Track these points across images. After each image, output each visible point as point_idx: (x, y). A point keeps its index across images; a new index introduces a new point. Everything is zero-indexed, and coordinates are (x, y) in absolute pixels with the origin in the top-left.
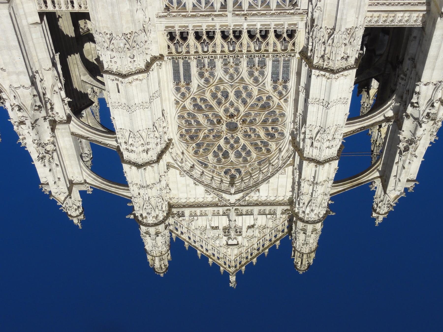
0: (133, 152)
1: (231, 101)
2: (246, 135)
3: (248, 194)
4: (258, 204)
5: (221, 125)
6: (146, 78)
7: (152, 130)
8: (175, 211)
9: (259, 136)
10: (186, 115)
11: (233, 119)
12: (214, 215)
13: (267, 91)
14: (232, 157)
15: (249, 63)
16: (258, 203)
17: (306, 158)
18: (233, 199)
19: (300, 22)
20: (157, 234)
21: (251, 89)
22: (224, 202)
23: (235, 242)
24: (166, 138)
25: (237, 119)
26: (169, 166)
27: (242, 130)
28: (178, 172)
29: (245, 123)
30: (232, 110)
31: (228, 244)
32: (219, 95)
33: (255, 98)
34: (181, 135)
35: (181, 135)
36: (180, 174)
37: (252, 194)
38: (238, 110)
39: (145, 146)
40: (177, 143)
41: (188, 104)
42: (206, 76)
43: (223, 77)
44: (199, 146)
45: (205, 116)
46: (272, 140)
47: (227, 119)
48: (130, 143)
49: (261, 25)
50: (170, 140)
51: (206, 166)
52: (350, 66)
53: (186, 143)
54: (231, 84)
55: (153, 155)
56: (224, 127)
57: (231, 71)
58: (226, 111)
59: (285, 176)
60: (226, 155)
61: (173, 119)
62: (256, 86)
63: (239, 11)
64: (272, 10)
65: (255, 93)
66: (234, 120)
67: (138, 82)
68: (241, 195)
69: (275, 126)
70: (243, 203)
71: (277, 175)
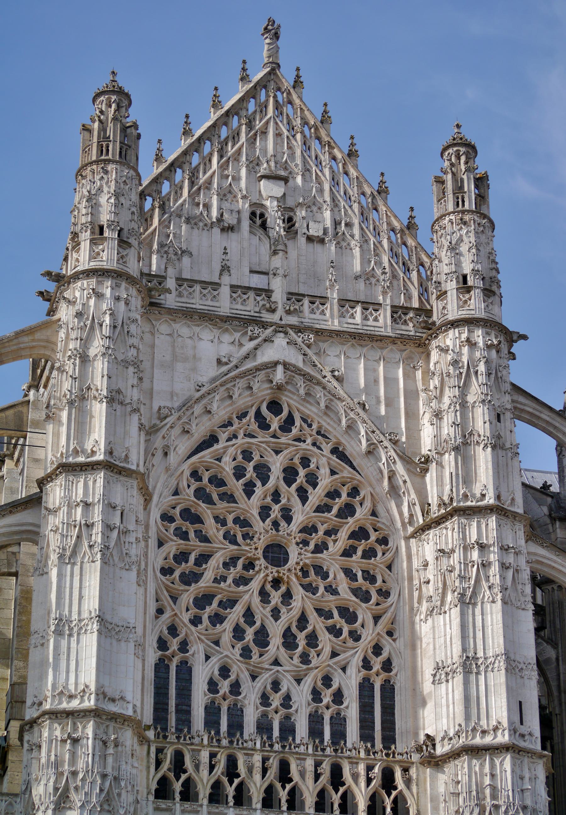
0: (506, 547)
2: (243, 523)
3: (247, 357)
4: (222, 320)
5: (301, 564)
9: (216, 518)
10: (374, 597)
11: (276, 575)
13: (202, 641)
15: (239, 713)
17: (134, 475)
22: (299, 340)
29: (248, 558)
32: (301, 639)
34: (384, 541)
38: (264, 595)
45: (334, 587)
46: (188, 503)
52: (57, 717)
53: (378, 522)
54: (279, 668)
56: (293, 552)
58: (288, 596)
62: (227, 656)
65: (227, 638)
66: (273, 572)
69: (182, 544)
70: (256, 332)
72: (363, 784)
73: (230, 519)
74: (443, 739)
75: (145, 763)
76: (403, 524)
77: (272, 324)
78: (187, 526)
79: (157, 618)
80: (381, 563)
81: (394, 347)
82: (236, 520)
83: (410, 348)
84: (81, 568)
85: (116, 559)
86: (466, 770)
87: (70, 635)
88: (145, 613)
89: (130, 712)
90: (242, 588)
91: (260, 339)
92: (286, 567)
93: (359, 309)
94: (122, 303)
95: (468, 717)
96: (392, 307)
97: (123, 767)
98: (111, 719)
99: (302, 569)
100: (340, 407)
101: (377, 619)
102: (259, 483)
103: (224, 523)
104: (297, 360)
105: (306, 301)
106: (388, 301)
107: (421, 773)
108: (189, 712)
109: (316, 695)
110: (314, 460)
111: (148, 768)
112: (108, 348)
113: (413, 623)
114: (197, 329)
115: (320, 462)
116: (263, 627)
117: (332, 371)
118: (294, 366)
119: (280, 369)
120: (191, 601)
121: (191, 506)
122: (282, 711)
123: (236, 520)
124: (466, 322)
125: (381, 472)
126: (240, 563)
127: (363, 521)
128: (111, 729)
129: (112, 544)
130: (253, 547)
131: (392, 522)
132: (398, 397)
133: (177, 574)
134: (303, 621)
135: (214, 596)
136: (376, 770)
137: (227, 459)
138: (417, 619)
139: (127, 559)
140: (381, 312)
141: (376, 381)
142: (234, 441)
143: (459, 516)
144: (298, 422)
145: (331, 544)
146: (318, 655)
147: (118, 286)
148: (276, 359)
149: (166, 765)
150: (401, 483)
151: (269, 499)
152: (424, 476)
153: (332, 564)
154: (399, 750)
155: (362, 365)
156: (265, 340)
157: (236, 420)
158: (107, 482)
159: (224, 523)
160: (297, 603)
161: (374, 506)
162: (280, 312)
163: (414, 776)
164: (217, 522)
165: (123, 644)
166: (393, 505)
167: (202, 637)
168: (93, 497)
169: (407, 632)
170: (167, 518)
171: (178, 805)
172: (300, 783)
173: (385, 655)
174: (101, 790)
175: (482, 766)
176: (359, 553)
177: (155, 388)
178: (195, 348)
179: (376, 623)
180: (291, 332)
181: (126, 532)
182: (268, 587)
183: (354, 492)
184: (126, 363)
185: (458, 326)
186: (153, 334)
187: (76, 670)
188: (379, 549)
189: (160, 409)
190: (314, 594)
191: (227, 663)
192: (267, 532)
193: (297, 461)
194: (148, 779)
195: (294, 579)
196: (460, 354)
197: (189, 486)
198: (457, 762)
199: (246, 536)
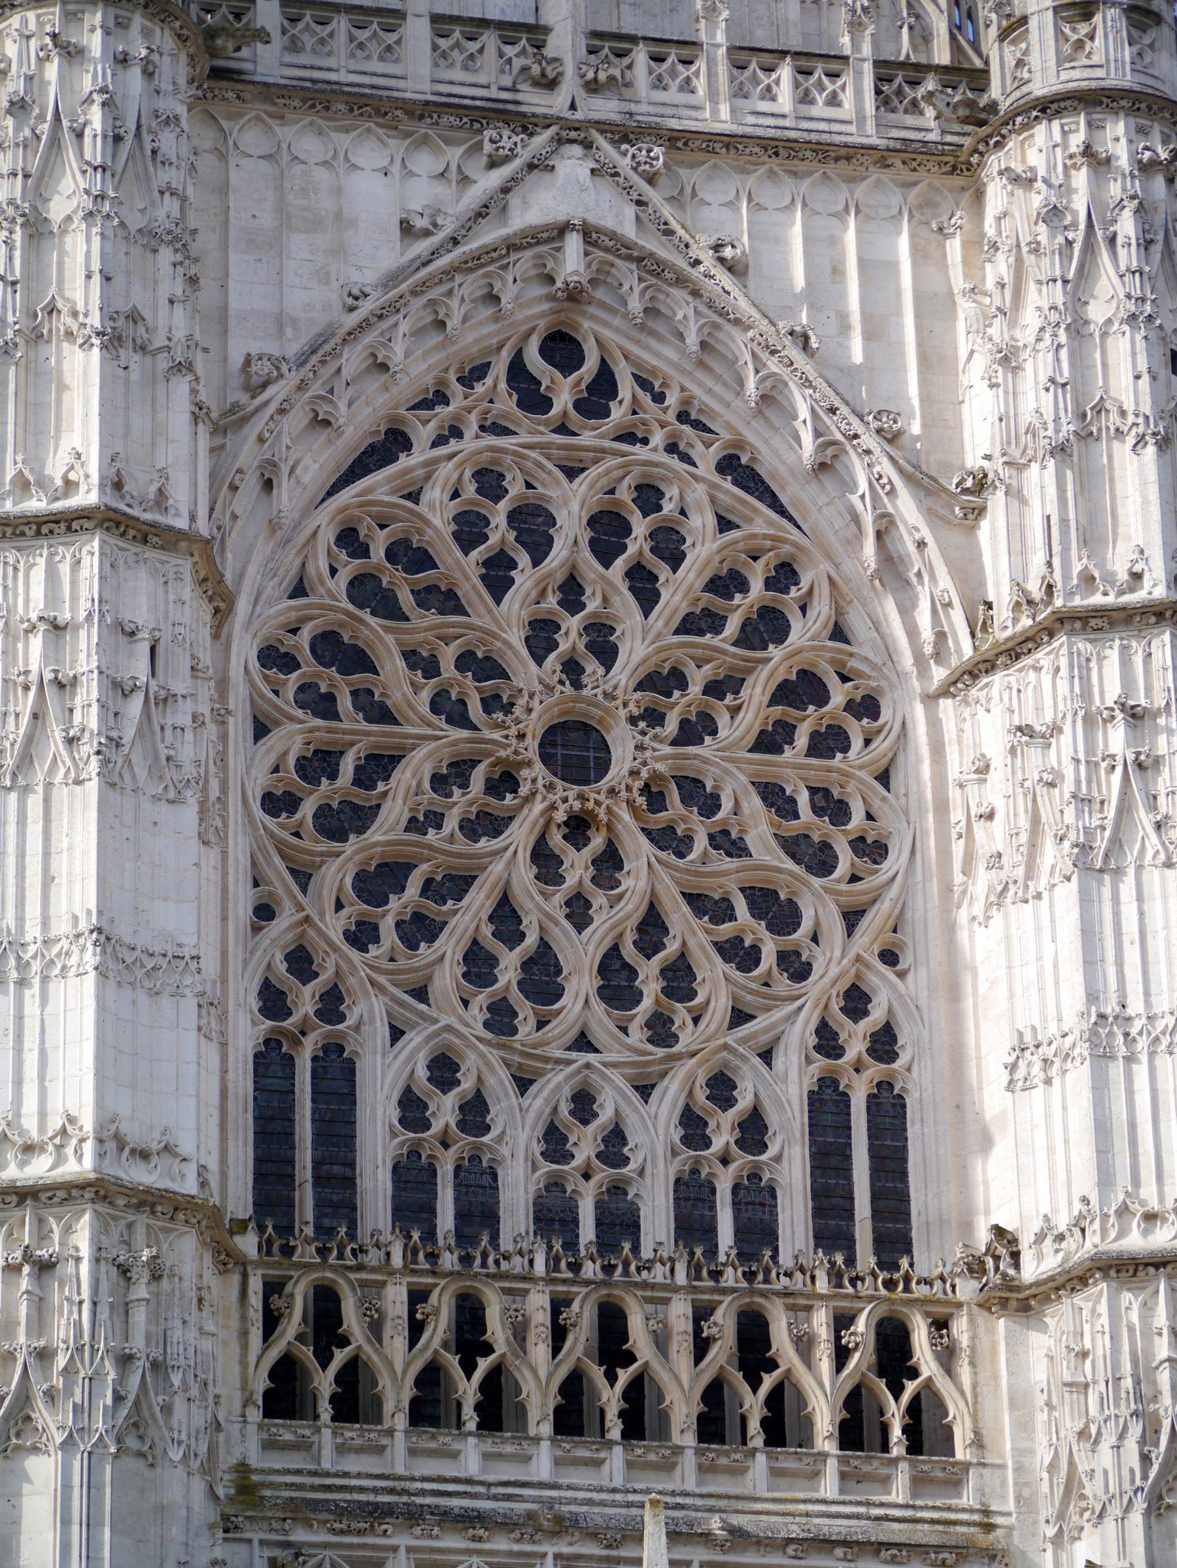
3: (481, 213)
4: (410, 114)
5: (644, 774)
9: (411, 657)
11: (577, 805)
15: (486, 1180)
16: (407, 124)
19: (254, 1461)
22: (625, 164)
25: (553, 807)
34: (867, 707)
35: (875, 715)
45: (734, 835)
46: (332, 615)
49: (454, 1455)
53: (851, 655)
54: (591, 1057)
62: (448, 1028)
64: (409, 1550)
69: (318, 729)
70: (506, 143)
72: (825, 1365)
73: (448, 656)
74: (1040, 1238)
75: (234, 1322)
76: (920, 661)
77: (548, 122)
78: (330, 679)
79: (256, 929)
80: (861, 767)
81: (885, 176)
82: (465, 661)
83: (930, 178)
84: (47, 800)
85: (141, 772)
86: (1105, 1320)
87: (22, 983)
88: (224, 919)
89: (190, 1186)
90: (484, 844)
91: (516, 164)
92: (604, 783)
93: (785, 72)
94: (136, 72)
95: (1105, 1179)
96: (877, 64)
97: (177, 1334)
98: (139, 1206)
99: (646, 789)
100: (740, 344)
101: (852, 917)
102: (523, 559)
103: (431, 668)
105: (640, 55)
106: (867, 50)
107: (981, 1331)
108: (349, 1182)
110: (671, 492)
111: (244, 1334)
112: (102, 197)
113: (950, 928)
114: (343, 140)
115: (690, 498)
116: (544, 946)
117: (717, 247)
118: (613, 236)
119: (573, 244)
120: (348, 881)
121: (342, 625)
122: (603, 1174)
123: (465, 661)
124: (1080, 100)
125: (856, 519)
126: (478, 776)
127: (810, 655)
128: (140, 1233)
129: (129, 734)
130: (513, 731)
131: (890, 654)
132: (899, 313)
133: (307, 810)
135: (409, 867)
136: (861, 1325)
137: (434, 494)
138: (963, 916)
139: (170, 773)
140: (847, 78)
141: (838, 272)
142: (453, 445)
143: (1072, 633)
144: (626, 388)
145: (723, 720)
146: (696, 1020)
147: (122, 24)
148: (561, 217)
149: (292, 1326)
150: (912, 548)
151: (552, 601)
152: (973, 529)
153: (727, 772)
154: (921, 1270)
155: (797, 230)
156: (531, 167)
157: (457, 388)
158: (110, 567)
159: (431, 668)
161: (839, 612)
162: (569, 86)
163: (964, 1340)
164: (412, 667)
165: (166, 1002)
166: (889, 608)
167: (382, 979)
168: (74, 608)
169: (936, 952)
171: (327, 1433)
172: (656, 1365)
173: (876, 1015)
174: (118, 1398)
175: (1147, 1309)
176: (802, 740)
177: (234, 303)
178: (338, 191)
179: (850, 929)
180: (600, 141)
181: (166, 700)
182: (556, 839)
184: (151, 239)
185: (1058, 113)
186: (223, 157)
187: (42, 1078)
188: (855, 729)
189: (248, 362)
190: (681, 855)
191: (449, 1047)
192: (550, 689)
193: (625, 494)
194: (244, 1364)
195: (626, 815)
196: (1065, 189)
197: (333, 571)
198: (1079, 1299)
199: (491, 703)
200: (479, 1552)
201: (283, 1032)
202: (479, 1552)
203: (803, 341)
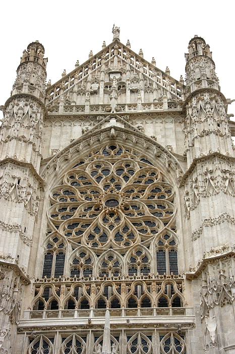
1: (111, 230)
2: (96, 192)
3: (96, 128)
6: (206, 253)
7: (201, 196)
8: (179, 109)
10: (164, 214)
12: (135, 105)
14: (113, 168)
18: (113, 122)
20: (199, 81)
21: (88, 244)
22: (122, 119)
23: (112, 76)
24: (187, 188)
26: (185, 159)
27: (100, 198)
28: (175, 151)
30: (112, 220)
31: (121, 73)
32: (125, 237)
33: (84, 234)
34: (170, 191)
36: (172, 149)
37: (90, 128)
38: (105, 220)
39: (210, 177)
40: (175, 184)
41: (162, 228)
42: (139, 258)
43: (120, 257)
44: (151, 181)
47: (117, 210)
48: (228, 181)
50: (182, 186)
51: (144, 159)
53: (165, 183)
55: (200, 169)
57: (111, 264)
58: (119, 219)
59: (51, 148)
60: (120, 170)
61: (179, 210)
63: (97, 331)
64: (59, 332)
65: (84, 238)
67: (216, 249)
68: (103, 128)
71: (61, 149)
89: (13, 263)
101: (165, 224)
104: (119, 125)
109: (133, 259)
119: (113, 131)
121: (69, 189)
127: (157, 185)
134: (126, 228)
145: (141, 197)
156: (106, 121)
160: (122, 221)
170: (55, 194)
183: (153, 174)
191: (84, 251)
200: (75, 332)
201: (50, 251)
202: (75, 332)
203: (154, 137)
